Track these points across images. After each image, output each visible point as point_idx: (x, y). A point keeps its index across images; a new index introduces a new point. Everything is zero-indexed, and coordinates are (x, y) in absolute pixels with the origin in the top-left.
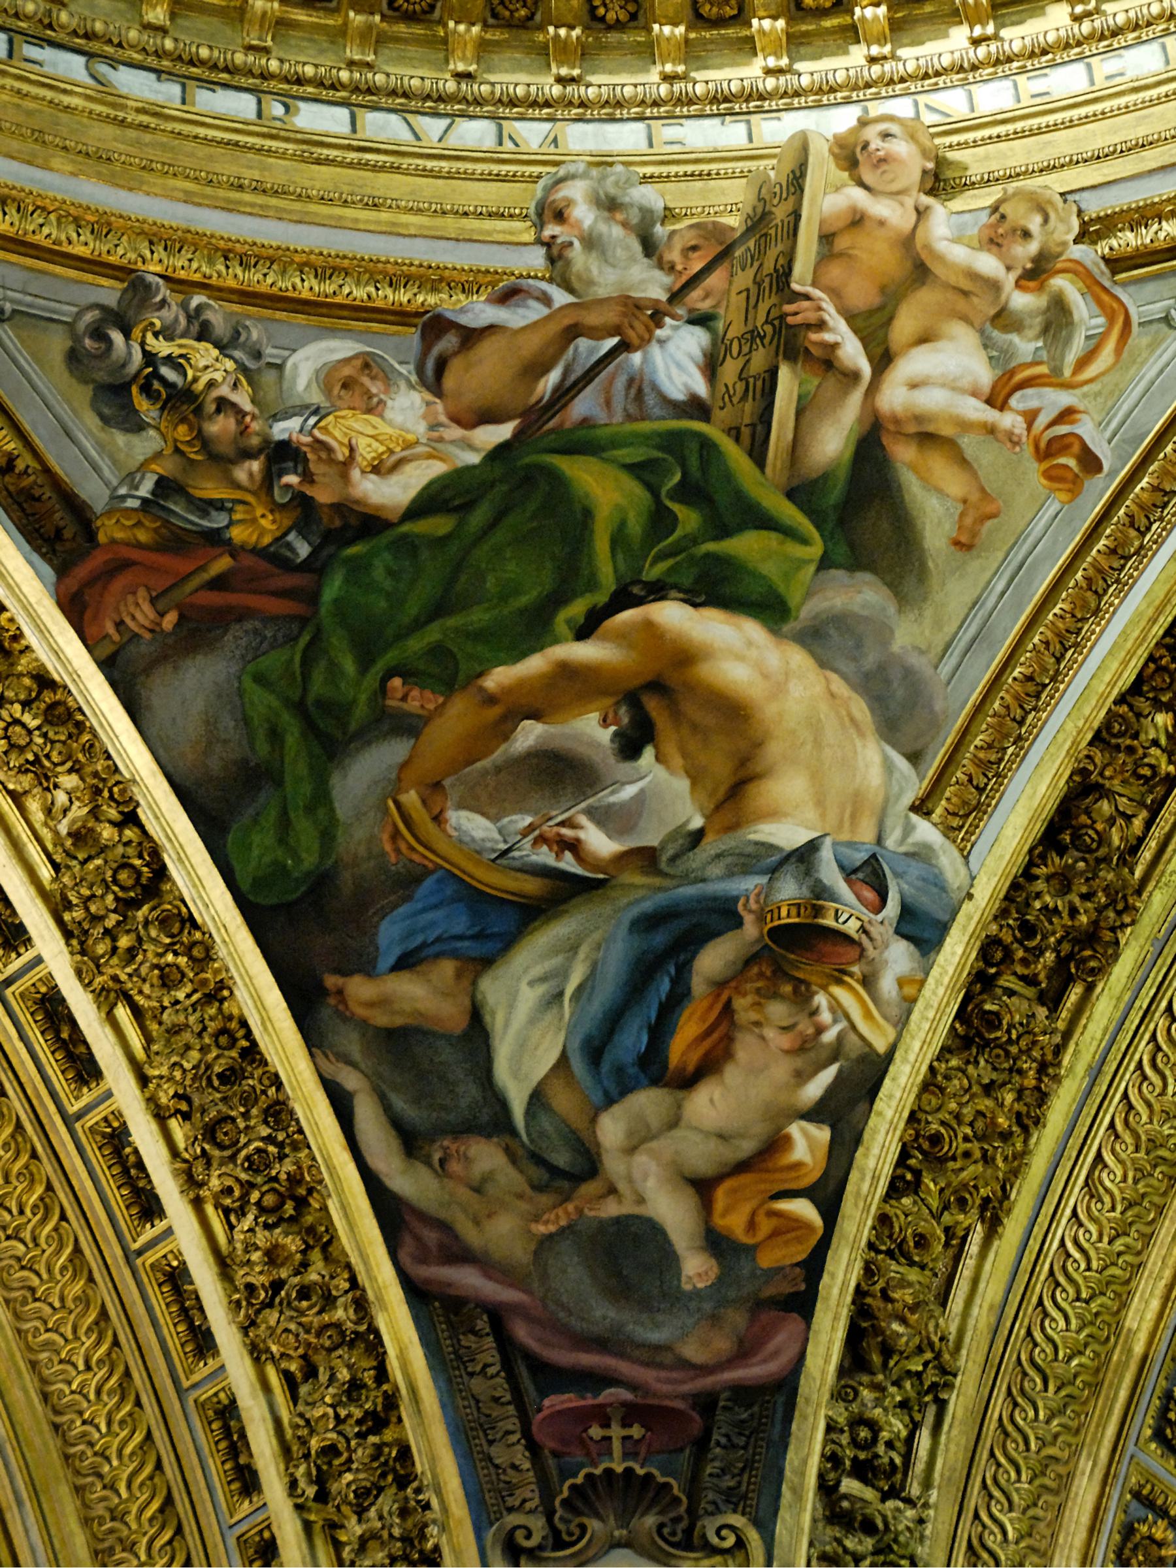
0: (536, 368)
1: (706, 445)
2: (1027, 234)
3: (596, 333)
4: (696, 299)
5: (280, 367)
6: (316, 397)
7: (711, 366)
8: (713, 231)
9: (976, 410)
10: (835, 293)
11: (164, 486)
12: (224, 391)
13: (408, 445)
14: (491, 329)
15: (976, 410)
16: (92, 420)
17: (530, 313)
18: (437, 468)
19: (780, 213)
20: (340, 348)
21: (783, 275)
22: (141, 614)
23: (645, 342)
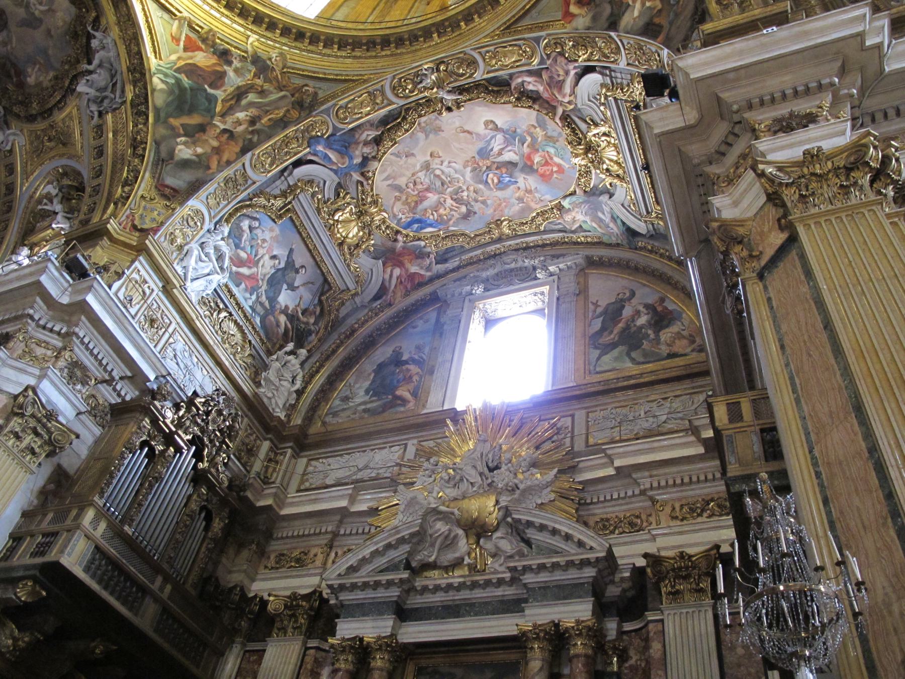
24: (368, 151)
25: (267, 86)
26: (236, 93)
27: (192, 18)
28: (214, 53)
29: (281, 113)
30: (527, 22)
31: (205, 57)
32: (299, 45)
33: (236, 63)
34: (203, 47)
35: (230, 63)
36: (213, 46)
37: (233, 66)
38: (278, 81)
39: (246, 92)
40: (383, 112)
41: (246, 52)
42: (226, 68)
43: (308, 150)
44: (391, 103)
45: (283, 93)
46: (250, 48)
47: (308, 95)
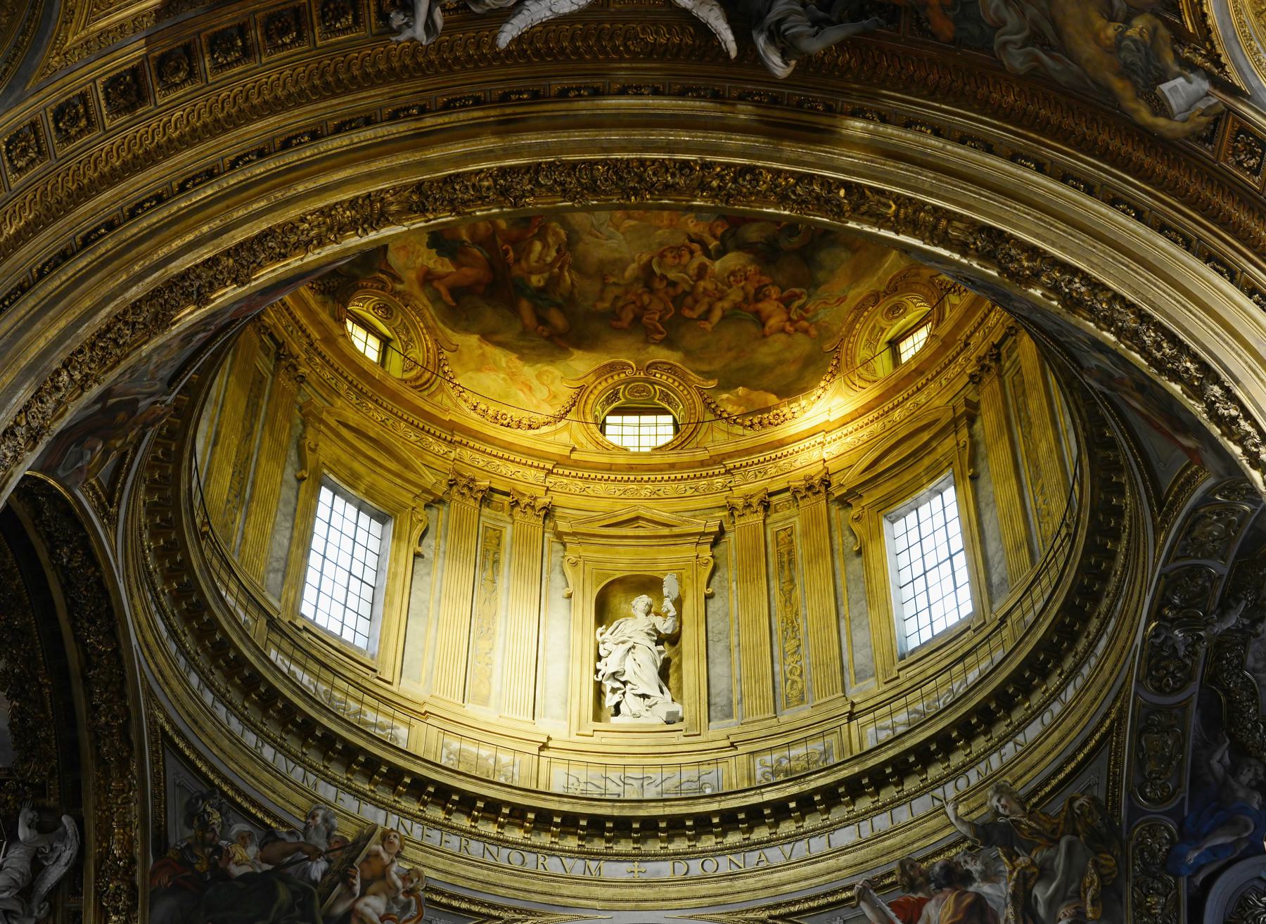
0: (286, 855)
1: (312, 895)
2: (412, 882)
3: (304, 853)
4: (331, 856)
5: (230, 826)
6: (234, 838)
7: (324, 874)
8: (344, 840)
9: (376, 918)
10: (362, 872)
11: (188, 846)
12: (215, 827)
13: (247, 860)
14: (283, 840)
15: (376, 918)
16: (182, 821)
17: (292, 840)
18: (250, 870)
19: (361, 844)
20: (246, 827)
21: (353, 860)
22: (165, 879)
23: (313, 860)
24: (1251, 775)
25: (1037, 856)
26: (1019, 909)
27: (869, 876)
28: (940, 887)
29: (1092, 877)
30: (1166, 483)
31: (937, 905)
32: (1001, 729)
33: (975, 867)
34: (921, 895)
35: (968, 878)
36: (928, 881)
37: (976, 875)
38: (1039, 833)
39: (1028, 893)
40: (1194, 719)
41: (965, 839)
42: (971, 889)
43: (1183, 882)
44: (1184, 706)
45: (1063, 844)
46: (964, 830)
47: (1090, 812)
